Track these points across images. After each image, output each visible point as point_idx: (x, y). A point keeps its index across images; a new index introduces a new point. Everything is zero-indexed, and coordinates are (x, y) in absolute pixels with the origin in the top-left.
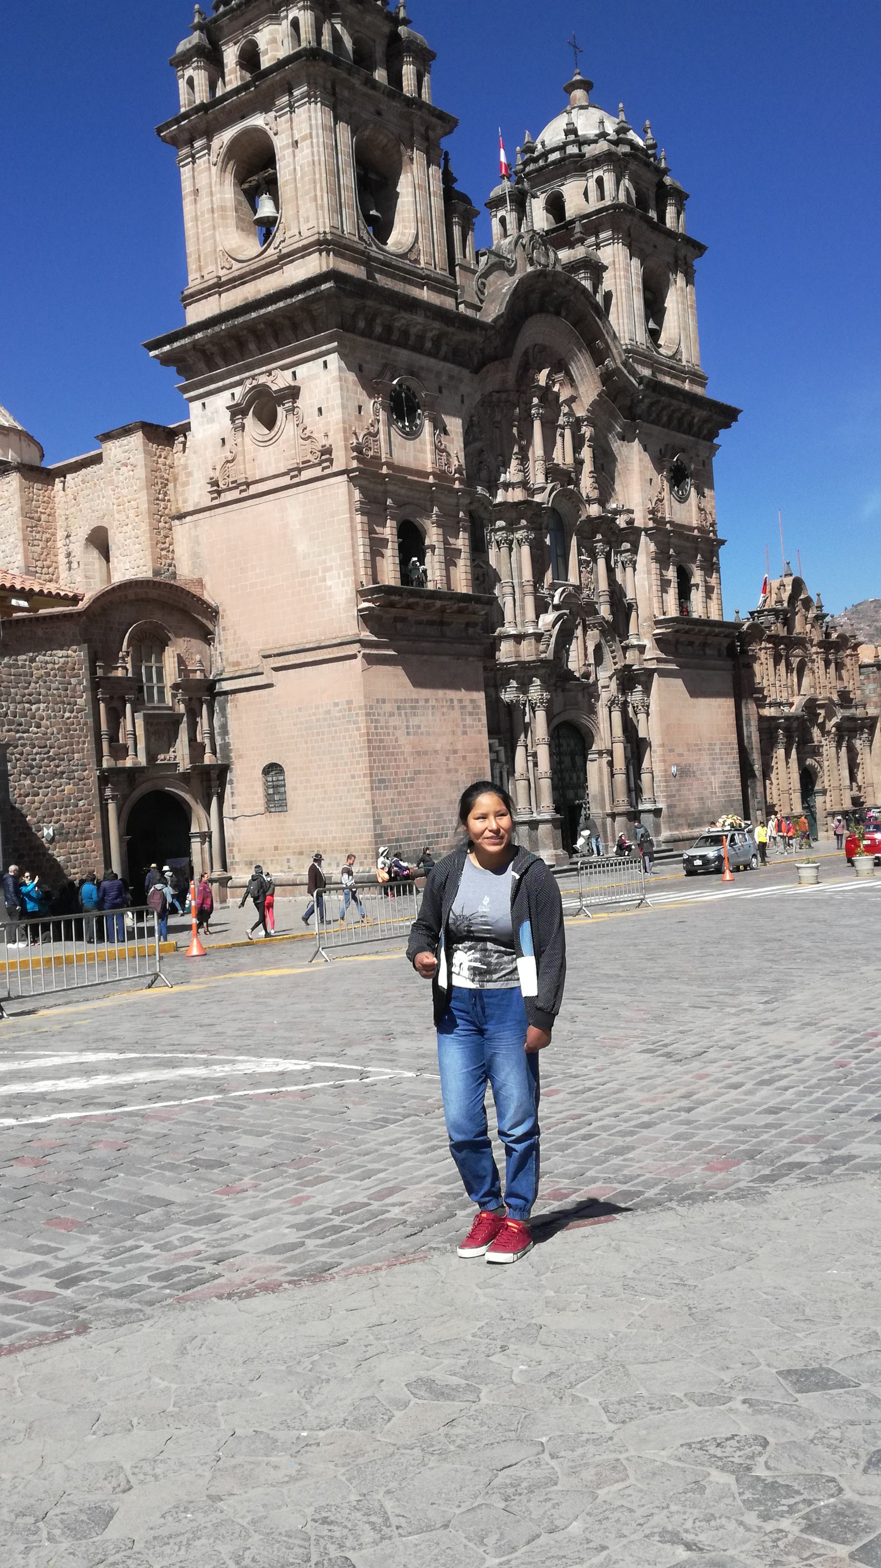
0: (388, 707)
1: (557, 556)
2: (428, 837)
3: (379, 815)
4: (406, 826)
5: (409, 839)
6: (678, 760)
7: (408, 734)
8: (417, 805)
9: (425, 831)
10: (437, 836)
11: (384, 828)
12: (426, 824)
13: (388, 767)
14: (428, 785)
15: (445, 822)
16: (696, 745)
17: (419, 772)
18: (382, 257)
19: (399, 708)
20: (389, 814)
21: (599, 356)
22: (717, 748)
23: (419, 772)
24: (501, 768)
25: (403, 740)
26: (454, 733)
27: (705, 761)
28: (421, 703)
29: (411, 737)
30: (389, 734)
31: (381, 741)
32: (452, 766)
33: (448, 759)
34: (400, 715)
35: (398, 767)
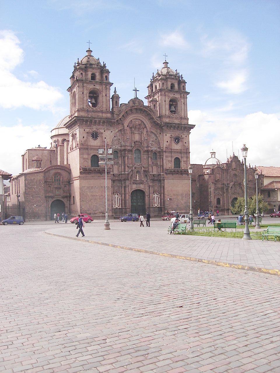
0: (85, 188)
1: (138, 158)
6: (170, 198)
11: (83, 208)
17: (92, 199)
22: (184, 195)
23: (92, 199)
25: (88, 194)
27: (180, 197)
32: (101, 198)
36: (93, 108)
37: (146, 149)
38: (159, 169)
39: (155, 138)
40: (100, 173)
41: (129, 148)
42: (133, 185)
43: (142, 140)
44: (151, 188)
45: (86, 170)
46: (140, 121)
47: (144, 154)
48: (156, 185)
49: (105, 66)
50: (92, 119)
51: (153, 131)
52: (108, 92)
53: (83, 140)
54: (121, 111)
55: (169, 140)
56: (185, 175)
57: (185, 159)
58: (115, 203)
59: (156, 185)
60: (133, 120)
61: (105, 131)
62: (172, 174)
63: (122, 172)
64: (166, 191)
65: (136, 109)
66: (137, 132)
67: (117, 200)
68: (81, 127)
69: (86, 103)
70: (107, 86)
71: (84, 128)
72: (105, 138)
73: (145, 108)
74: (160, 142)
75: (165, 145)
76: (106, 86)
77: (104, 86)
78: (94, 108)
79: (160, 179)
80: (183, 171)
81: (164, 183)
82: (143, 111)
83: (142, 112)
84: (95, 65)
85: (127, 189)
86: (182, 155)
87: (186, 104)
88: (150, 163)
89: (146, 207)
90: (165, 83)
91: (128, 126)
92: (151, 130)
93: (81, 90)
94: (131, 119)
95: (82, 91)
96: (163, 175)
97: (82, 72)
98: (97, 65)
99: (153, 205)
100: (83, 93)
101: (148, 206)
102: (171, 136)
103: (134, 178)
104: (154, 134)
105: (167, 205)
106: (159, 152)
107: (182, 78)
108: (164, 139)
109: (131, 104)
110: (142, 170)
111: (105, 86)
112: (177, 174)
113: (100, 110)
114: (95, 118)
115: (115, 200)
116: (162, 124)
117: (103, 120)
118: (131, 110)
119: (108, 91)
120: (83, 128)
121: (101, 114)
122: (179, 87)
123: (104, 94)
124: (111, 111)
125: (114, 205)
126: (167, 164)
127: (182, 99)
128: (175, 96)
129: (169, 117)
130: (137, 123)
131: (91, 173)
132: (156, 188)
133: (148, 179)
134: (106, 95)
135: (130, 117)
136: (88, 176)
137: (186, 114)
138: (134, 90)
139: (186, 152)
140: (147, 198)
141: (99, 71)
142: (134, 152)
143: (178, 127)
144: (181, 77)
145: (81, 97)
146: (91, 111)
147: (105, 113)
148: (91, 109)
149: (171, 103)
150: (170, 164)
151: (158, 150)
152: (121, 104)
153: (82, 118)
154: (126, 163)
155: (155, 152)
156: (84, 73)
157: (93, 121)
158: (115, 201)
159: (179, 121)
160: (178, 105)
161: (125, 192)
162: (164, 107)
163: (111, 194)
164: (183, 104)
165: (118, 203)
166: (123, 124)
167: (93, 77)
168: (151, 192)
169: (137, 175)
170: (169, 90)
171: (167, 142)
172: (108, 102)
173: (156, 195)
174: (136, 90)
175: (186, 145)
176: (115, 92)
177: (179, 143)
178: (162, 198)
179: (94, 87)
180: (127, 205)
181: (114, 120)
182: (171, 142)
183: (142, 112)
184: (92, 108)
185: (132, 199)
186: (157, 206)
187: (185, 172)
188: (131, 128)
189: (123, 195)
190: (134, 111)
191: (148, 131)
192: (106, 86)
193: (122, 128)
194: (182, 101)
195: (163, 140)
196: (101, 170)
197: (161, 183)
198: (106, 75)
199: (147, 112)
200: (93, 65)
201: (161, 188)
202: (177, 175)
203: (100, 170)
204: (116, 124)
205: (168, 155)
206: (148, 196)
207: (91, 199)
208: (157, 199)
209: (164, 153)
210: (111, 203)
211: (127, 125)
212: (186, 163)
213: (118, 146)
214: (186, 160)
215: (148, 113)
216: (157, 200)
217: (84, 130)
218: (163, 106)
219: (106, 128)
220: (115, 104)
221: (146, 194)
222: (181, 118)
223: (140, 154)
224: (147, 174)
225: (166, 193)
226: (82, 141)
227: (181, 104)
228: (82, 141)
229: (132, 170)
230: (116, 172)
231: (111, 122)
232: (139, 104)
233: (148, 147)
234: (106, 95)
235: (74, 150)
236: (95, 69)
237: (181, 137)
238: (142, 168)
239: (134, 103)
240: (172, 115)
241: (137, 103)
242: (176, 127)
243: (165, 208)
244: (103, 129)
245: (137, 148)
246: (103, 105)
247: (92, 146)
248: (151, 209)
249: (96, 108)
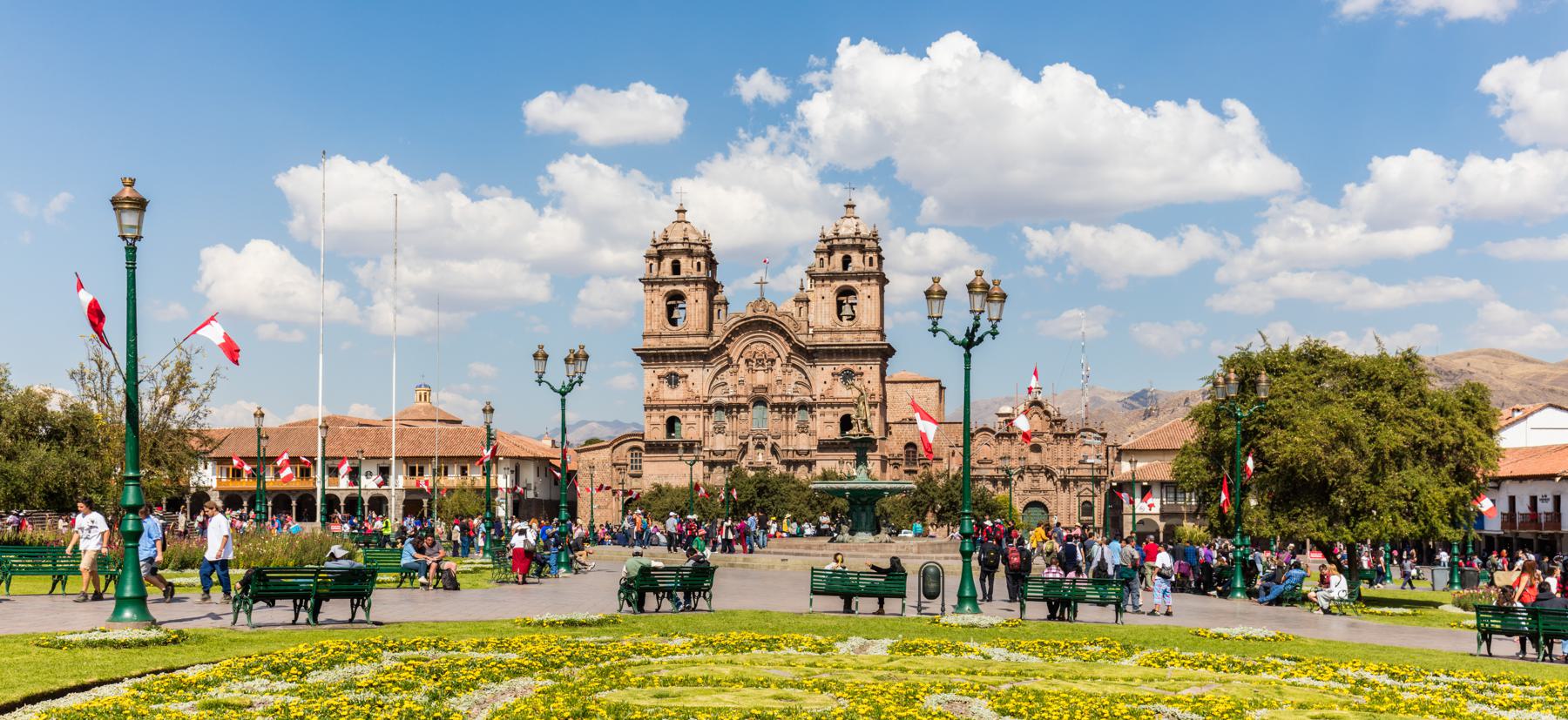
21: (789, 339)
37: (777, 400)
41: (742, 400)
75: (818, 390)
78: (675, 328)
90: (826, 259)
94: (748, 342)
108: (818, 377)
123: (693, 301)
129: (831, 331)
159: (856, 335)
167: (676, 268)
230: (720, 447)
238: (769, 438)
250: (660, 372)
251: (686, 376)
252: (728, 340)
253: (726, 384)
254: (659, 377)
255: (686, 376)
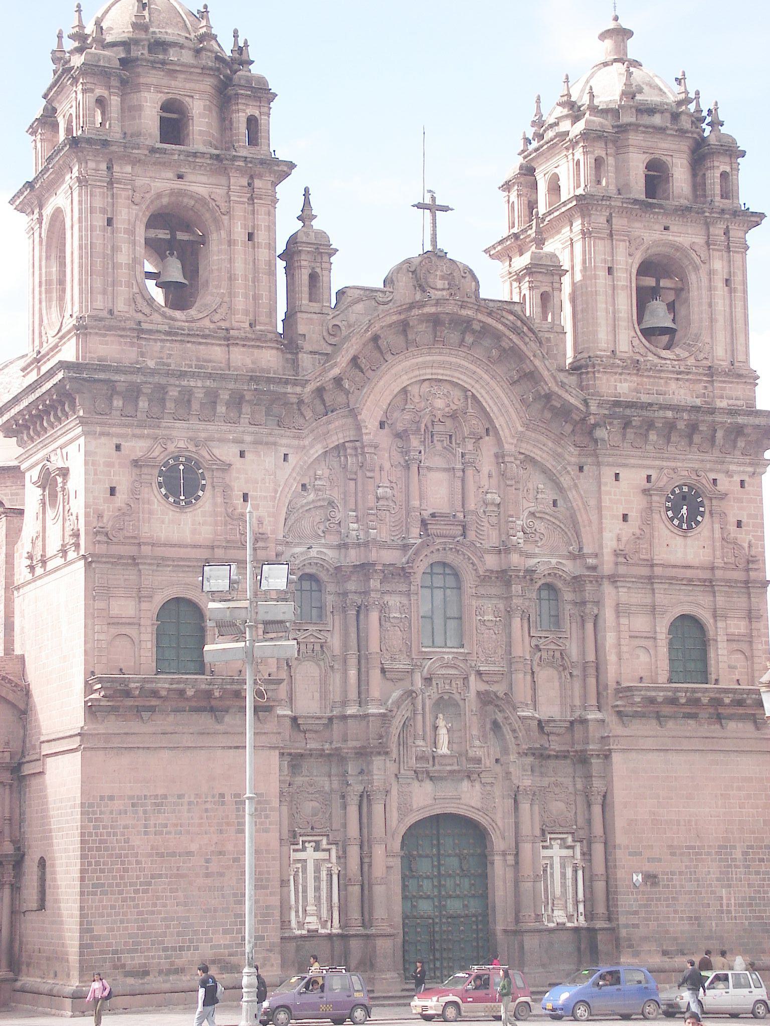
0: (117, 804)
1: (446, 618)
2: (165, 949)
3: (89, 923)
4: (130, 936)
5: (136, 951)
7: (146, 833)
8: (153, 913)
9: (163, 942)
10: (181, 949)
11: (97, 938)
12: (164, 934)
13: (111, 871)
14: (171, 891)
15: (195, 932)
16: (693, 847)
17: (160, 876)
18: (167, 328)
19: (133, 805)
20: (107, 922)
22: (738, 854)
23: (160, 876)
24: (330, 870)
25: (136, 841)
26: (221, 832)
28: (170, 799)
29: (152, 837)
30: (115, 834)
31: (101, 842)
32: (214, 867)
33: (207, 861)
34: (136, 812)
35: (126, 870)
36: (169, 312)
37: (491, 562)
38: (577, 686)
39: (549, 495)
40: (212, 710)
42: (416, 784)
43: (471, 505)
44: (525, 807)
45: (127, 694)
46: (457, 394)
47: (482, 591)
48: (556, 785)
49: (241, 58)
50: (163, 381)
51: (537, 454)
52: (262, 220)
53: (109, 509)
54: (344, 332)
55: (635, 505)
56: (740, 725)
57: (738, 626)
58: (305, 898)
59: (557, 790)
60: (414, 390)
61: (242, 454)
62: (658, 717)
63: (344, 703)
64: (620, 823)
65: (435, 321)
66: (438, 462)
67: (317, 879)
68: (98, 429)
69: (129, 285)
70: (260, 176)
71: (118, 436)
72: (245, 497)
73: (490, 314)
74: (581, 518)
76: (252, 177)
77: (239, 181)
78: (178, 314)
79: (578, 747)
80: (727, 701)
81: (607, 776)
82: (473, 332)
83: (469, 339)
84: (182, 47)
85: (378, 809)
86: (721, 600)
87: (740, 288)
88: (521, 648)
89: (499, 928)
90: (611, 160)
91: (382, 425)
92: (526, 448)
93: (98, 203)
94: (404, 381)
95: (103, 211)
96: (603, 721)
97: (105, 93)
98: (198, 52)
99: (538, 918)
100: (110, 222)
101: (511, 918)
102: (648, 485)
103: (420, 742)
104: (545, 471)
105: (628, 913)
106: (575, 578)
107: (716, 124)
109: (405, 291)
110: (472, 695)
111: (244, 181)
112: (694, 716)
113: (212, 326)
114: (182, 375)
115: (305, 879)
116: (593, 409)
117: (231, 386)
118: (404, 327)
119: (263, 210)
120: (108, 434)
121: (218, 349)
122: (699, 179)
123: (239, 232)
124: (280, 330)
125: (293, 914)
126: (625, 656)
127: (717, 254)
128: (669, 237)
130: (439, 403)
131: (152, 709)
132: (557, 807)
133: (505, 751)
134: (250, 236)
135: (393, 371)
136: (135, 726)
137: (741, 348)
138: (419, 206)
139: (747, 582)
140: (500, 870)
141: (207, 85)
142: (417, 579)
143: (693, 428)
144: (708, 119)
145: (98, 249)
146: (158, 331)
147: (245, 342)
148: (156, 317)
149: (650, 282)
150: (643, 657)
151: (570, 567)
152: (341, 293)
153: (102, 376)
154: (374, 646)
155: (549, 580)
156: (115, 101)
157: (173, 393)
158: (305, 891)
159: (699, 387)
160: (694, 294)
161: (365, 831)
162: (601, 306)
163: (275, 843)
164: (720, 284)
165: (318, 899)
166: (353, 413)
168: (526, 829)
169: (441, 723)
170: (636, 201)
171: (625, 517)
172: (264, 278)
173: (557, 852)
174: (433, 208)
175: (744, 537)
176: (306, 216)
177: (698, 523)
178: (599, 867)
179: (178, 185)
180: (380, 913)
181: (298, 389)
182: (647, 521)
183: (469, 339)
184: (164, 315)
185: (409, 873)
186: (565, 920)
187: (740, 703)
188: (400, 436)
189: (354, 852)
190: (422, 331)
191: (503, 457)
192: (252, 177)
193: (351, 434)
194: (718, 265)
195: (600, 509)
196: (217, 694)
197: (589, 777)
198: (250, 111)
199: (498, 336)
200: (171, 51)
201: (589, 805)
202: (691, 722)
203: (209, 694)
204: (308, 414)
205: (633, 601)
206: (510, 859)
207: (153, 877)
208: (563, 875)
209: (608, 589)
210: (275, 901)
211: (379, 415)
212: (744, 647)
213: (325, 546)
214: (743, 631)
215: (505, 344)
216: (564, 885)
217: (118, 447)
218: (601, 298)
219: (248, 438)
220: (306, 289)
221: (499, 843)
222: (711, 372)
223: (460, 596)
224: (499, 717)
225: (620, 838)
226: (100, 516)
227: (710, 289)
228: (100, 516)
229: (410, 694)
231: (279, 399)
232: (453, 286)
233: (504, 549)
234: (250, 236)
235: (50, 565)
236: (181, 76)
237: (710, 486)
238: (472, 678)
239: (421, 287)
240: (651, 357)
241: (439, 286)
242: (681, 425)
243: (617, 939)
244: (236, 441)
245: (436, 557)
246: (232, 294)
247: (165, 545)
248: (531, 942)
249: (193, 312)
250: (136, 447)
251: (226, 467)
252: (354, 361)
253: (331, 503)
254: (136, 463)
255: (226, 467)
